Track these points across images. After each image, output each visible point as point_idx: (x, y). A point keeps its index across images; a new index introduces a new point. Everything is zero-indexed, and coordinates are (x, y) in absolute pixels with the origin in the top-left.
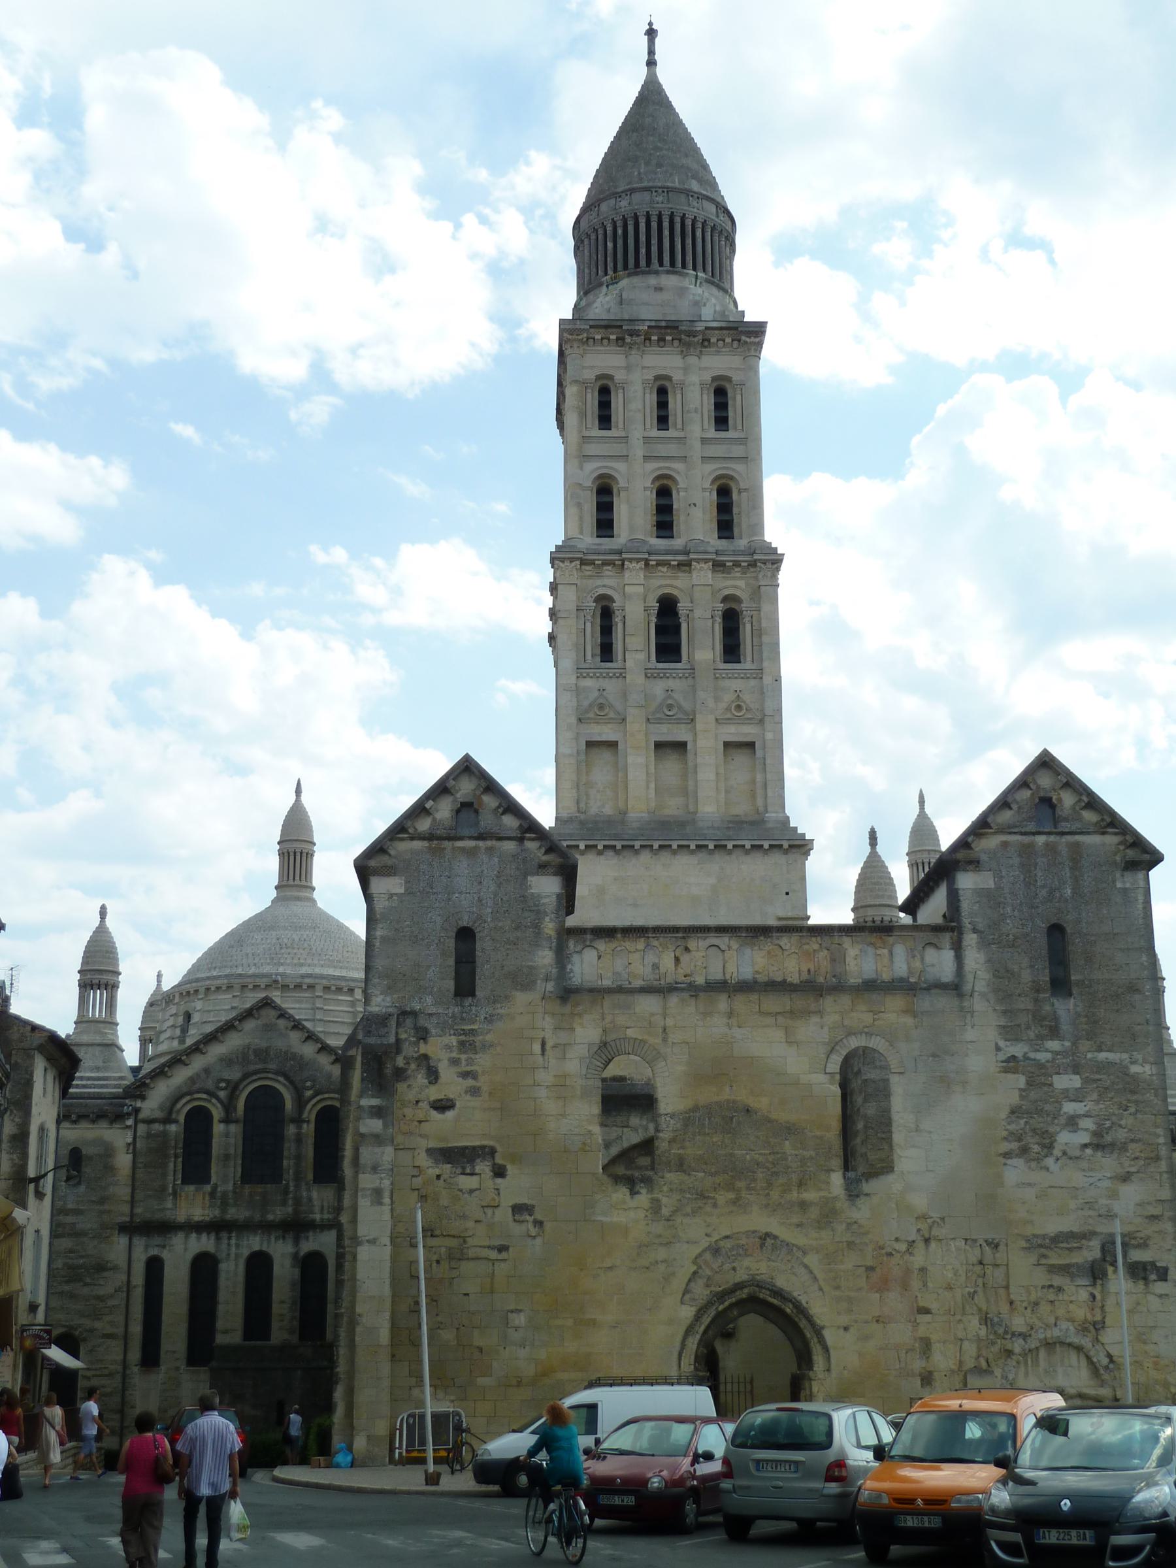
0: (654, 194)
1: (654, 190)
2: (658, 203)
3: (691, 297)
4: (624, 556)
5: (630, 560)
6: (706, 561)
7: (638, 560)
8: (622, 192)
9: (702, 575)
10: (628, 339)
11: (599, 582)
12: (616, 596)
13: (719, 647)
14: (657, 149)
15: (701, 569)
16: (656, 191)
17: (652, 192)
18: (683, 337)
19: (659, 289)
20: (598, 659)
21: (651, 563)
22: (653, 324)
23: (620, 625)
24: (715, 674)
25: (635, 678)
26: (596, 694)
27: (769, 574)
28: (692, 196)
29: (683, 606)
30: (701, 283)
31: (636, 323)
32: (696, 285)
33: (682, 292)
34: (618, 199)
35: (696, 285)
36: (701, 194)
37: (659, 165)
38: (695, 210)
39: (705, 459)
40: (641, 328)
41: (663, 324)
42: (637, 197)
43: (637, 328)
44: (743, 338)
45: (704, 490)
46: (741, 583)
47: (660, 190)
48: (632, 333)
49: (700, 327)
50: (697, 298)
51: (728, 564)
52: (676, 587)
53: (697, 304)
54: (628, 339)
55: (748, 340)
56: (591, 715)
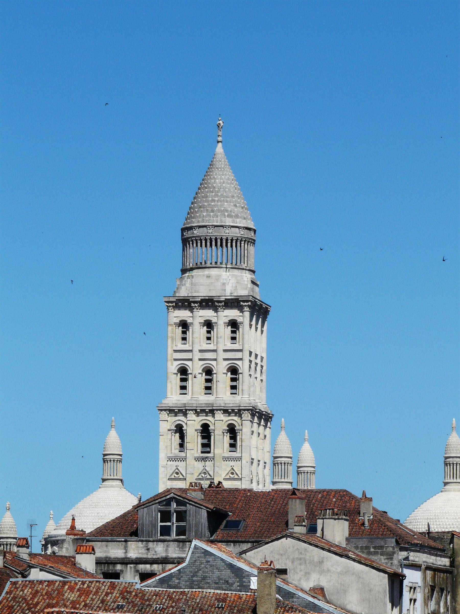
0: (208, 228)
1: (208, 227)
2: (210, 233)
3: (222, 281)
4: (186, 408)
5: (189, 410)
6: (220, 410)
7: (192, 410)
8: (196, 226)
9: (219, 416)
10: (193, 305)
11: (177, 418)
12: (184, 425)
13: (227, 445)
14: (213, 201)
15: (219, 413)
16: (209, 227)
17: (207, 227)
18: (216, 303)
19: (208, 277)
20: (177, 451)
21: (198, 410)
22: (203, 298)
23: (186, 437)
24: (223, 459)
25: (191, 460)
26: (175, 468)
27: (246, 415)
28: (226, 227)
29: (211, 427)
30: (229, 270)
31: (196, 298)
32: (226, 272)
33: (218, 278)
34: (194, 230)
35: (226, 272)
36: (230, 226)
37: (213, 211)
38: (227, 234)
39: (225, 359)
40: (197, 300)
41: (207, 298)
42: (201, 229)
43: (196, 300)
44: (241, 303)
45: (224, 373)
46: (236, 418)
47: (211, 227)
48: (195, 302)
49: (223, 299)
50: (225, 281)
51: (229, 410)
52: (208, 420)
53: (224, 284)
54: (193, 305)
55: (243, 304)
56: (173, 477)
